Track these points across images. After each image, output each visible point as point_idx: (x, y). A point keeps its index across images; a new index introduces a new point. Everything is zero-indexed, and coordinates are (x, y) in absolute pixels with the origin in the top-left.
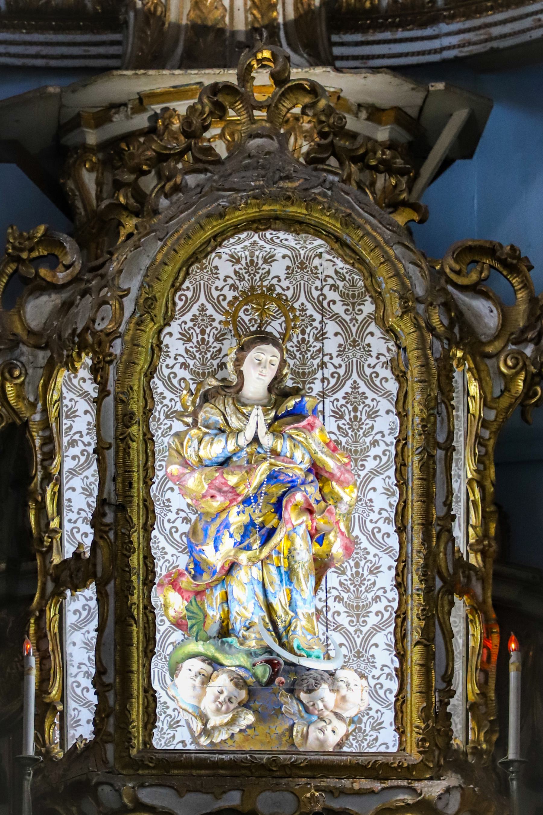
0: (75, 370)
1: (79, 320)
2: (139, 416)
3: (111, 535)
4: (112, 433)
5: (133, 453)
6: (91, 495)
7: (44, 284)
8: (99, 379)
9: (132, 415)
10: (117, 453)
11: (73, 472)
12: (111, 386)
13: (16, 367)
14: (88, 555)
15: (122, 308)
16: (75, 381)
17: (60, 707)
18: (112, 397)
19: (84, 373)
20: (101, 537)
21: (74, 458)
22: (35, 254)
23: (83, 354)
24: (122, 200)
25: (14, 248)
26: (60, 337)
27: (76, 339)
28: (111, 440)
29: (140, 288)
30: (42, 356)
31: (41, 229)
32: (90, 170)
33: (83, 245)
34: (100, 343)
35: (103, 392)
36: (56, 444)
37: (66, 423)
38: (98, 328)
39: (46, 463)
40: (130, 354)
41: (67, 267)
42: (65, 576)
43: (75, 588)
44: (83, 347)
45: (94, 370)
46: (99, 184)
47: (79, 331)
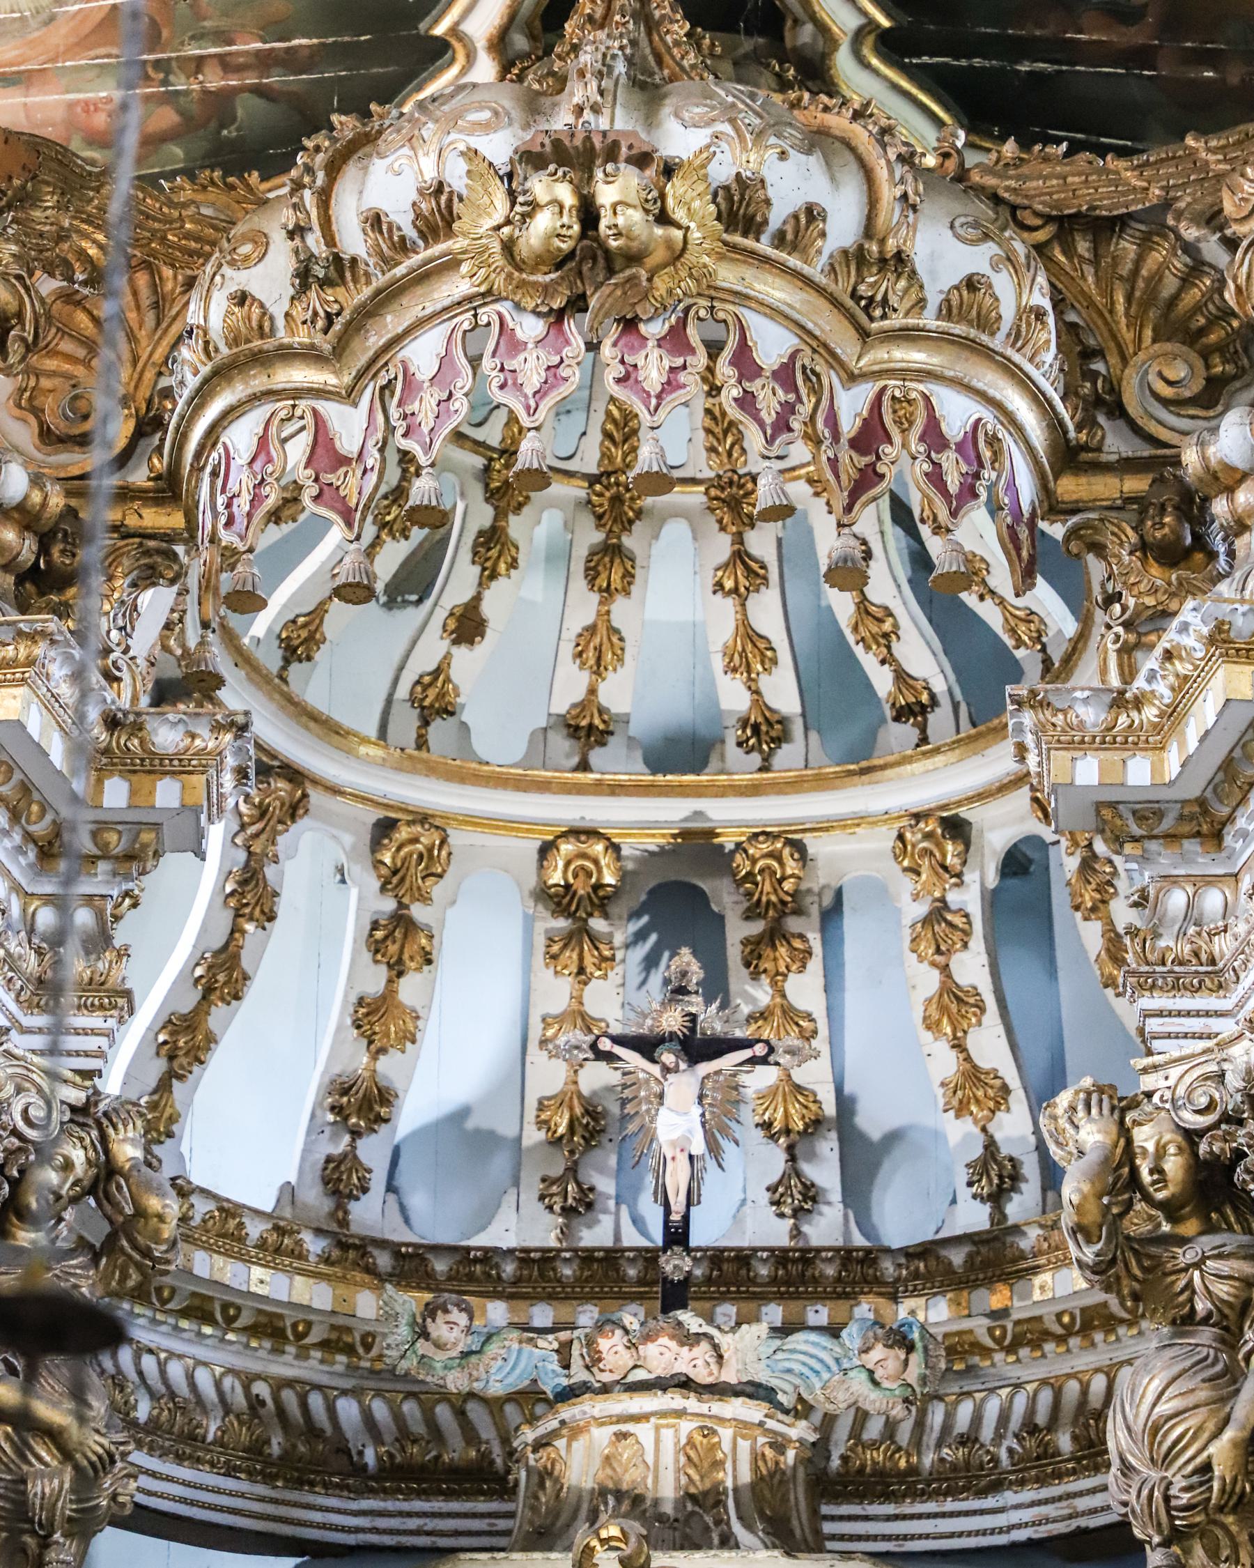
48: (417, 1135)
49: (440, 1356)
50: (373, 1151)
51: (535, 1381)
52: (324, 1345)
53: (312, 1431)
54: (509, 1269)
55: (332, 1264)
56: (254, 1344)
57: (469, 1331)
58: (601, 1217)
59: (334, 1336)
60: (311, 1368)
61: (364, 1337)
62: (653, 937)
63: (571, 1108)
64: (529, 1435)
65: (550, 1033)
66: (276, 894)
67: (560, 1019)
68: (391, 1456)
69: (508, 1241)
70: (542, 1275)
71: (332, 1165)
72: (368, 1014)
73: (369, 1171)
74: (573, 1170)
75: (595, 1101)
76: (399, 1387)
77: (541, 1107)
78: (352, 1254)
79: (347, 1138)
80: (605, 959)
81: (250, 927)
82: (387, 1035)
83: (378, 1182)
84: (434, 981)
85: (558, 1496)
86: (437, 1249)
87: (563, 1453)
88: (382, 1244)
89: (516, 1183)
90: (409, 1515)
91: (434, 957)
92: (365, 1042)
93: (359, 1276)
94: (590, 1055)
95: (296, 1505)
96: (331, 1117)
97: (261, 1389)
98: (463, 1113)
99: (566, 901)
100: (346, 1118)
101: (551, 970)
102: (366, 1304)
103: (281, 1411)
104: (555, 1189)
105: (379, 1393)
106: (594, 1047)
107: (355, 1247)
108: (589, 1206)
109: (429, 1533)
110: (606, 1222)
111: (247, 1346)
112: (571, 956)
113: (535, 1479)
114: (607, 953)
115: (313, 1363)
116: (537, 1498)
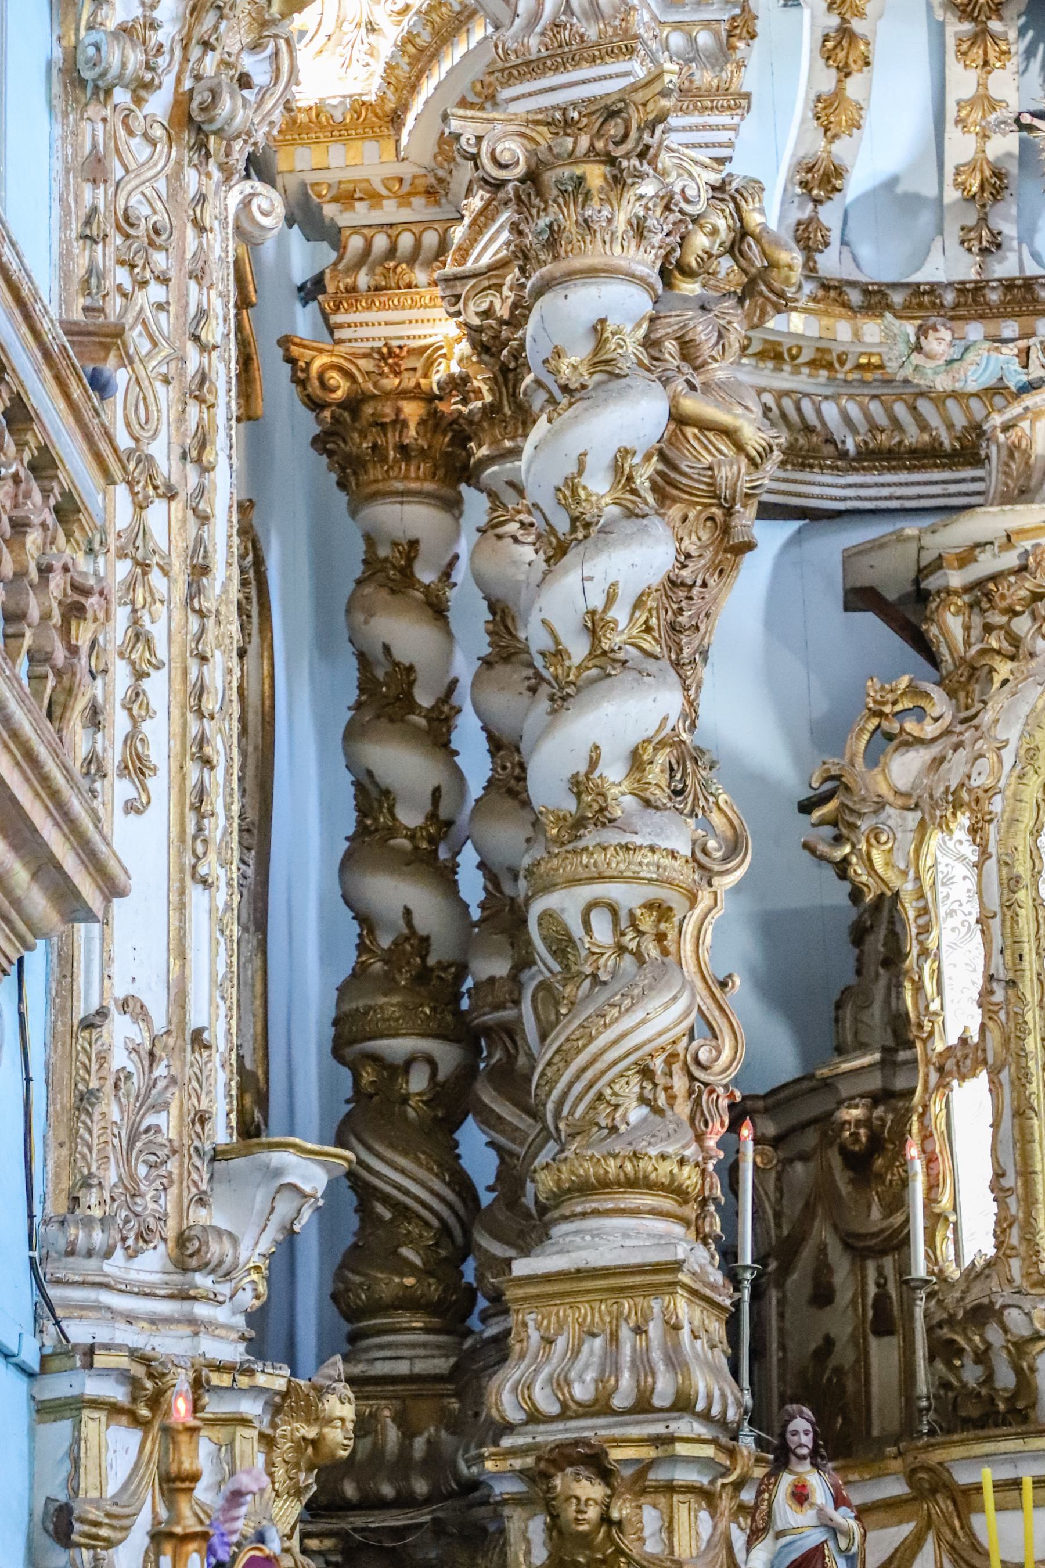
0: (950, 831)
1: (952, 777)
2: (1026, 879)
3: (1002, 1015)
4: (996, 900)
5: (1022, 921)
6: (975, 970)
7: (911, 739)
8: (978, 840)
9: (1018, 879)
10: (1003, 921)
11: (953, 946)
12: (992, 848)
13: (882, 831)
14: (976, 1039)
15: (1000, 761)
16: (951, 844)
17: (952, 1218)
18: (994, 859)
19: (961, 834)
20: (990, 1018)
21: (953, 930)
22: (898, 707)
23: (959, 814)
24: (995, 644)
25: (875, 702)
26: (931, 797)
27: (950, 798)
28: (996, 908)
29: (1021, 738)
30: (912, 819)
31: (904, 681)
32: (956, 614)
33: (952, 694)
34: (977, 801)
35: (985, 854)
36: (933, 915)
37: (942, 891)
38: (974, 783)
39: (921, 937)
40: (1013, 811)
41: (936, 720)
42: (950, 1065)
43: (963, 1078)
44: (958, 805)
45: (973, 831)
46: (967, 628)
47: (952, 789)
48: (858, 200)
49: (930, 364)
50: (830, 215)
51: (1001, 379)
52: (812, 364)
53: (808, 429)
54: (949, 298)
55: (818, 302)
56: (761, 365)
57: (951, 345)
58: (1009, 254)
59: (819, 356)
60: (802, 381)
61: (839, 357)
62: (1030, 34)
63: (982, 172)
64: (997, 419)
65: (963, 113)
66: (756, 17)
67: (972, 103)
68: (866, 443)
69: (941, 277)
70: (974, 300)
71: (802, 227)
72: (824, 108)
73: (829, 230)
74: (984, 219)
75: (999, 165)
76: (866, 391)
77: (958, 173)
78: (832, 294)
79: (811, 206)
80: (1004, 53)
81: (741, 45)
82: (840, 123)
83: (835, 237)
84: (871, 80)
85: (1027, 463)
86: (895, 286)
87: (1028, 432)
88: (853, 284)
89: (941, 231)
90: (883, 485)
91: (870, 60)
92: (822, 130)
93: (838, 310)
94: (1015, 128)
95: (801, 482)
96: (798, 191)
97: (768, 399)
98: (892, 182)
99: (969, 9)
100: (810, 191)
101: (962, 65)
102: (843, 330)
103: (784, 415)
104: (972, 235)
105: (851, 397)
106: (1017, 121)
107: (835, 288)
108: (999, 246)
109: (898, 498)
110: (1012, 258)
111: (756, 367)
112: (977, 52)
113: (1004, 452)
114: (1004, 48)
115: (803, 377)
116: (1007, 465)
